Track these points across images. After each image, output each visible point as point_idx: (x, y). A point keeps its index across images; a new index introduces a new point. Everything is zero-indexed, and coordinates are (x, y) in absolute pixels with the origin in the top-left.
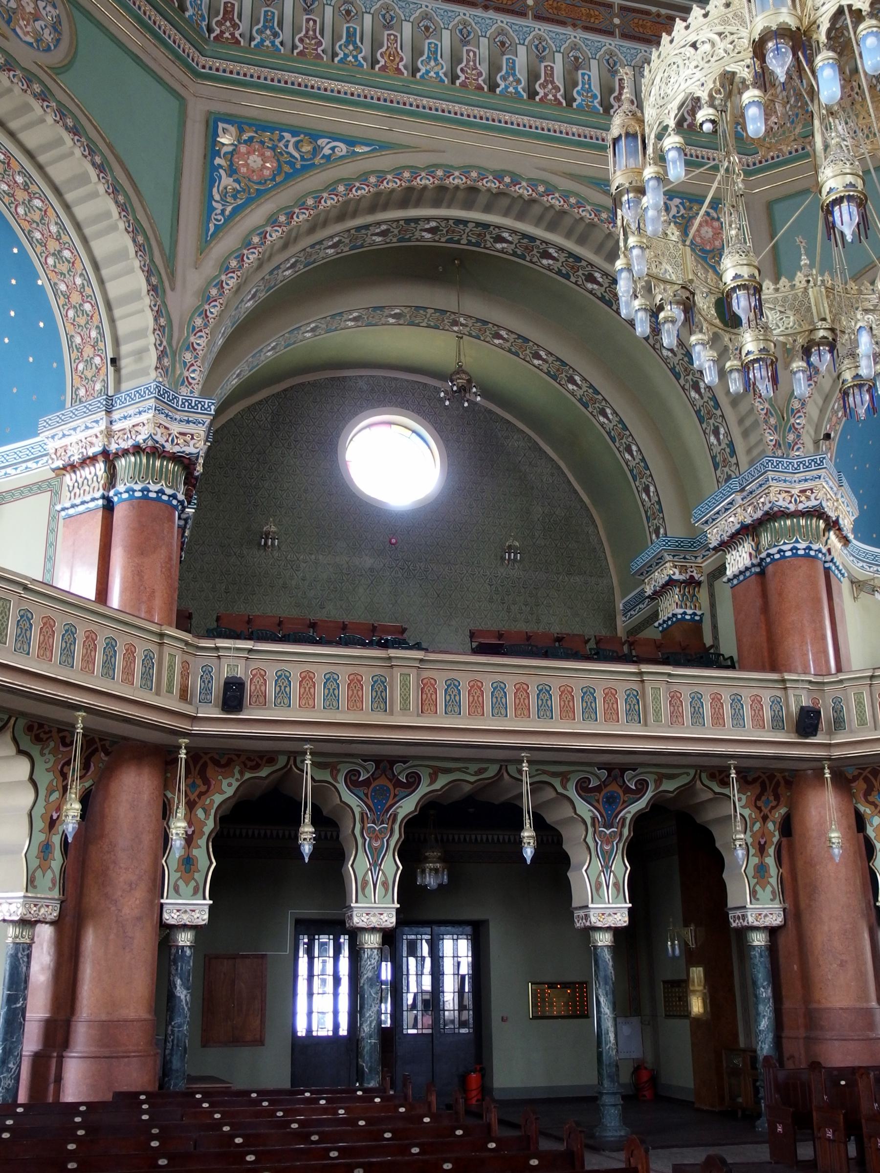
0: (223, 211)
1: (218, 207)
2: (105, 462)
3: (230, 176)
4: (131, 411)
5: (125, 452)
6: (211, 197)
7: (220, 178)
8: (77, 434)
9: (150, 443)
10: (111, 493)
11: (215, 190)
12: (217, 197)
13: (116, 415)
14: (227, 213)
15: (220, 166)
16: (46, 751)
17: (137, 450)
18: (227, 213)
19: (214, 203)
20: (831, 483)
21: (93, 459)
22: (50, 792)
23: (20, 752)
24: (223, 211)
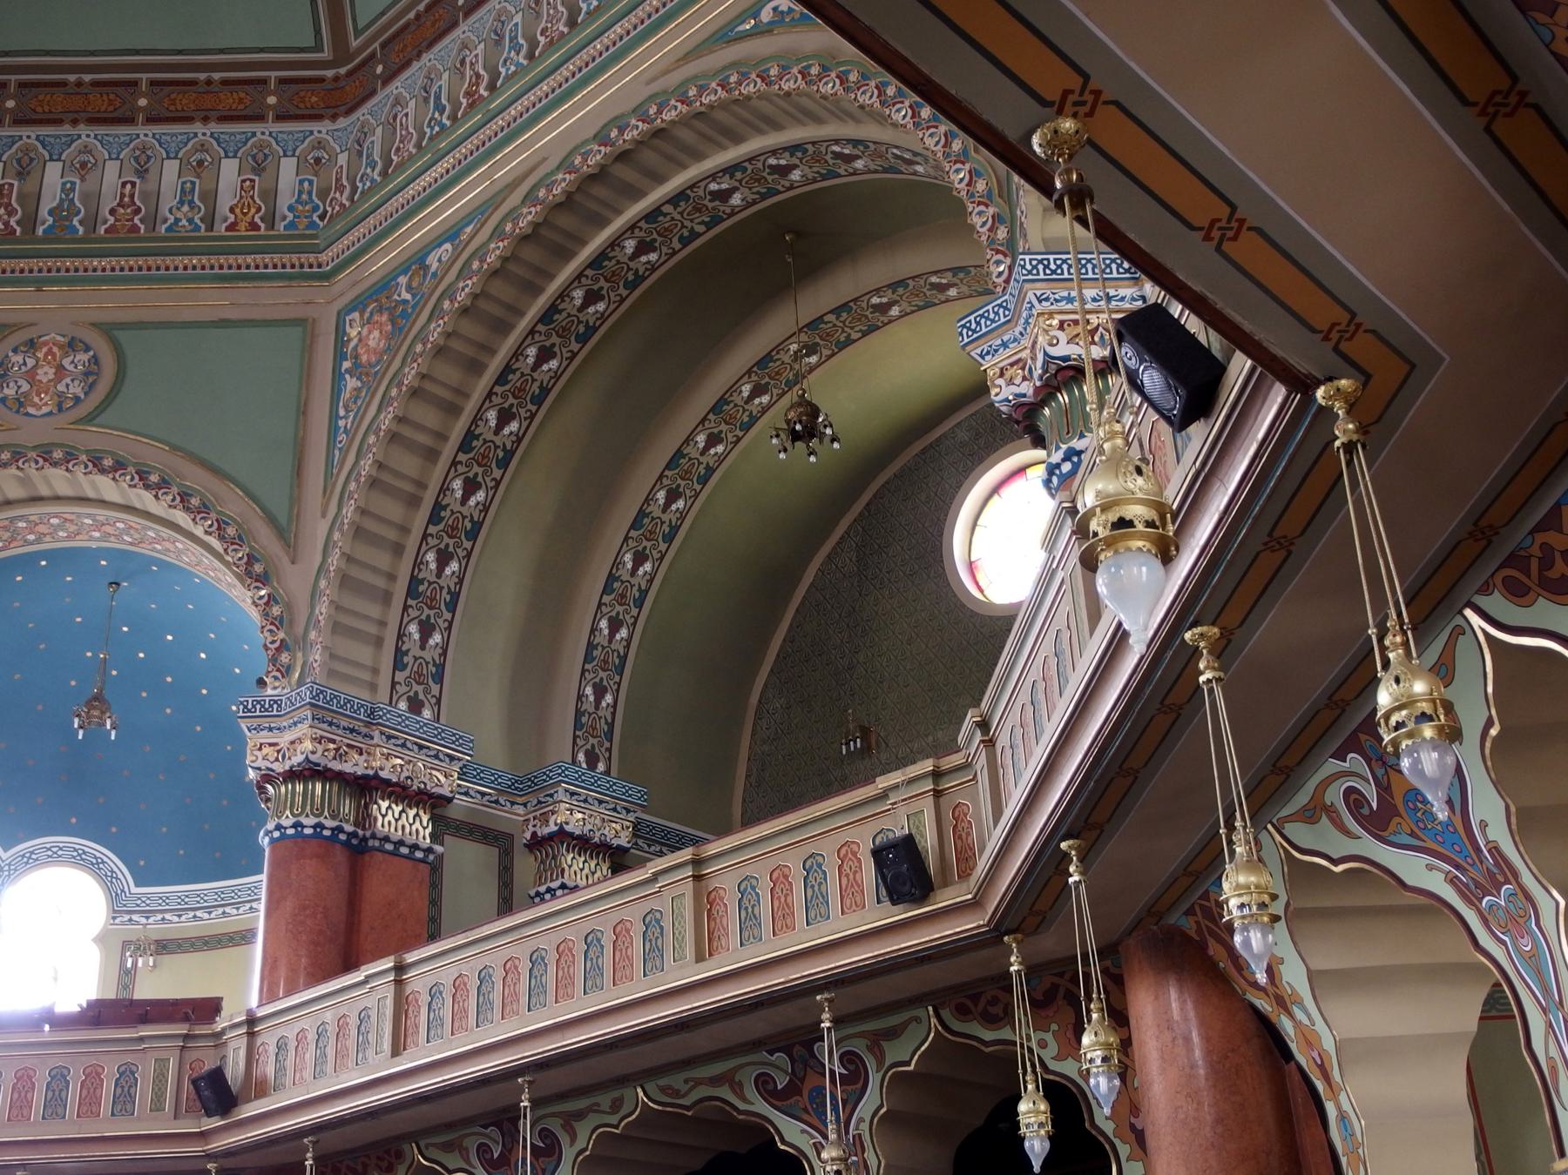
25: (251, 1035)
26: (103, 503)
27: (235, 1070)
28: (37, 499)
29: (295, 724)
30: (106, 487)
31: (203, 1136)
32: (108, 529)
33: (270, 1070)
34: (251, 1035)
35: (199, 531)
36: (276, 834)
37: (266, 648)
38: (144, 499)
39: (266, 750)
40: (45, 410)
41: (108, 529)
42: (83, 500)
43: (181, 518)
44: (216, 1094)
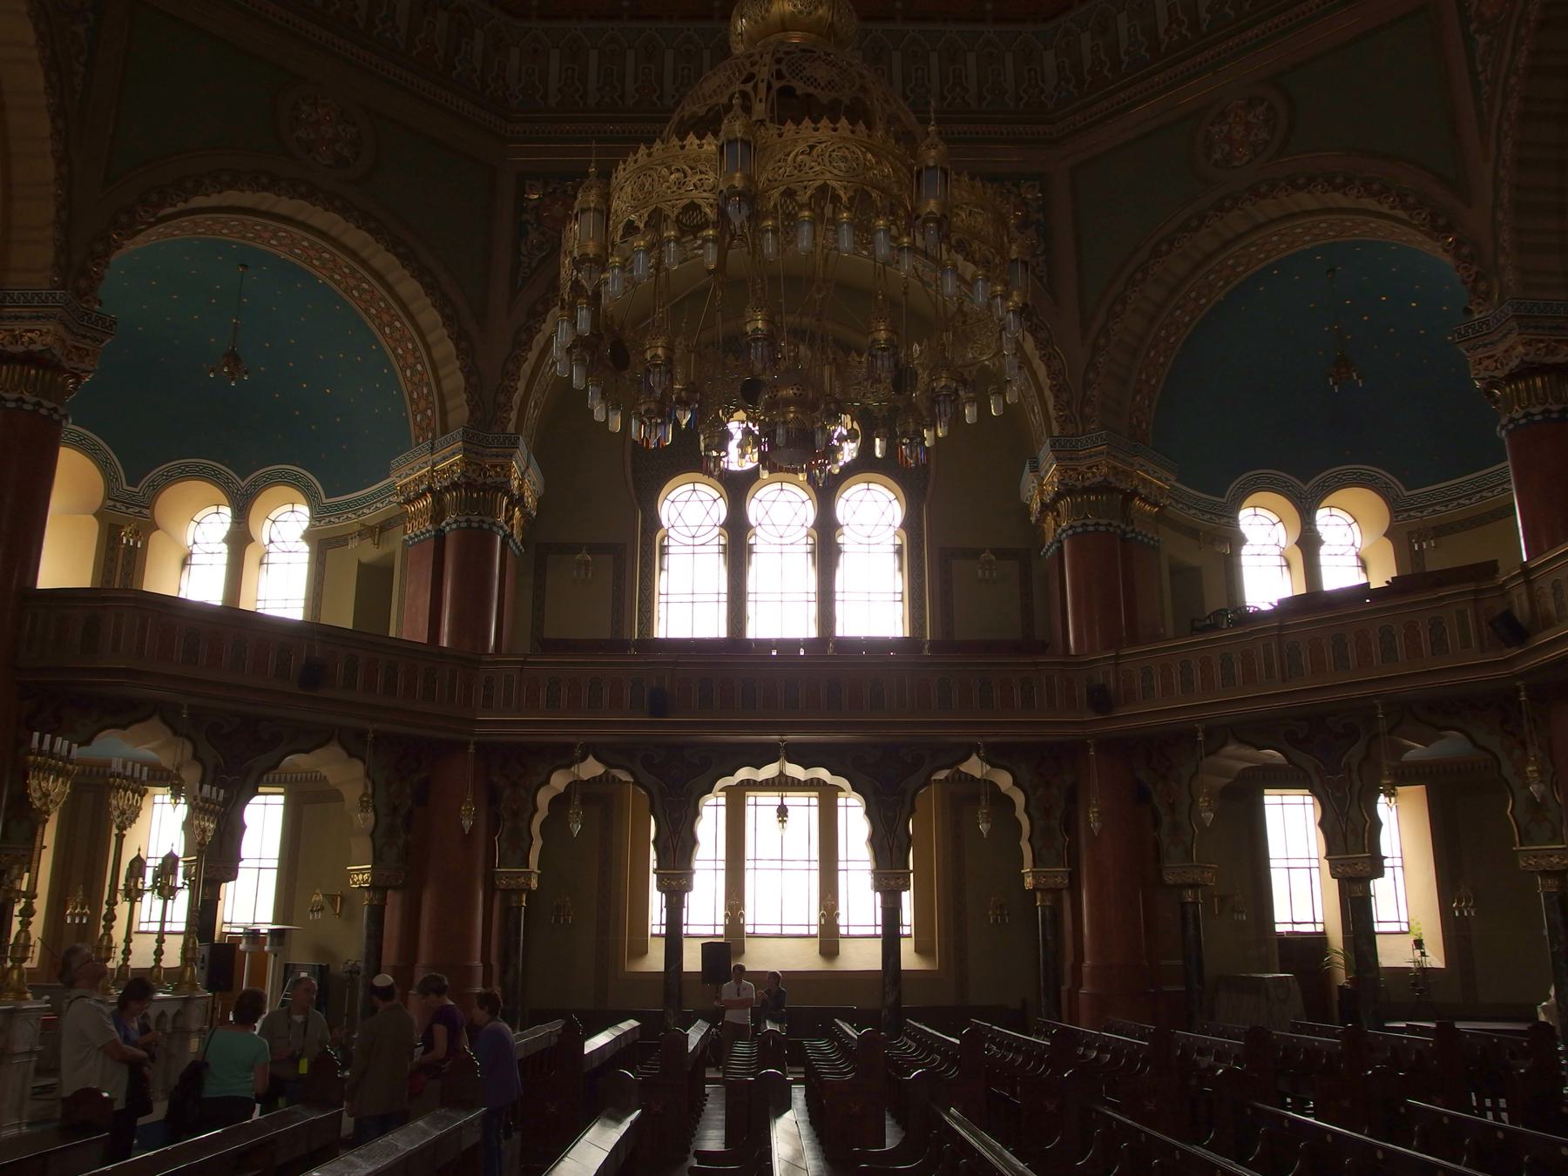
8: (410, 471)
17: (455, 486)
21: (423, 495)
25: (1529, 583)
26: (1311, 213)
27: (1520, 605)
28: (1258, 227)
29: (1505, 336)
30: (1306, 200)
31: (1508, 662)
32: (1316, 231)
33: (1551, 606)
34: (1529, 583)
35: (1385, 209)
36: (1511, 426)
37: (1464, 283)
38: (1338, 199)
39: (1485, 363)
40: (1246, 159)
41: (1316, 231)
42: (1291, 216)
43: (1369, 203)
44: (1512, 630)
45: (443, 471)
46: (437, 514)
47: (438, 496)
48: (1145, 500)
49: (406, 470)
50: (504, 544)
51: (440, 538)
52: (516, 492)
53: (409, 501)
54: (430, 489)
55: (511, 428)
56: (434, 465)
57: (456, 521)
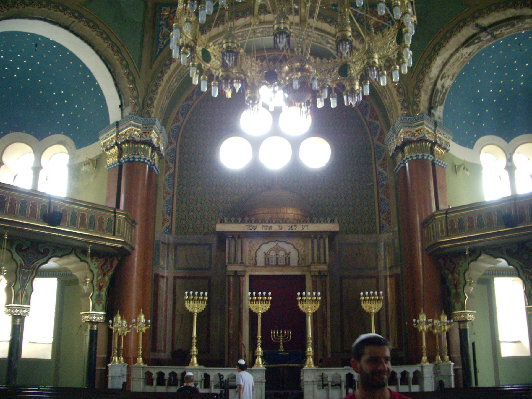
0: (163, 43)
1: (161, 41)
2: (118, 147)
3: (167, 27)
4: (124, 127)
5: (123, 143)
6: (158, 38)
7: (162, 29)
8: (108, 137)
9: (131, 139)
10: (122, 159)
11: (160, 34)
12: (161, 37)
13: (120, 129)
14: (165, 43)
15: (163, 24)
16: (94, 260)
17: (127, 141)
18: (165, 43)
19: (160, 40)
20: (430, 126)
21: (113, 147)
22: (98, 275)
23: (82, 261)
24: (163, 43)
45: (122, 135)
46: (120, 156)
47: (119, 146)
48: (440, 146)
49: (105, 135)
50: (151, 170)
51: (120, 166)
52: (156, 145)
53: (107, 150)
54: (116, 144)
55: (153, 116)
56: (119, 132)
57: (128, 158)
